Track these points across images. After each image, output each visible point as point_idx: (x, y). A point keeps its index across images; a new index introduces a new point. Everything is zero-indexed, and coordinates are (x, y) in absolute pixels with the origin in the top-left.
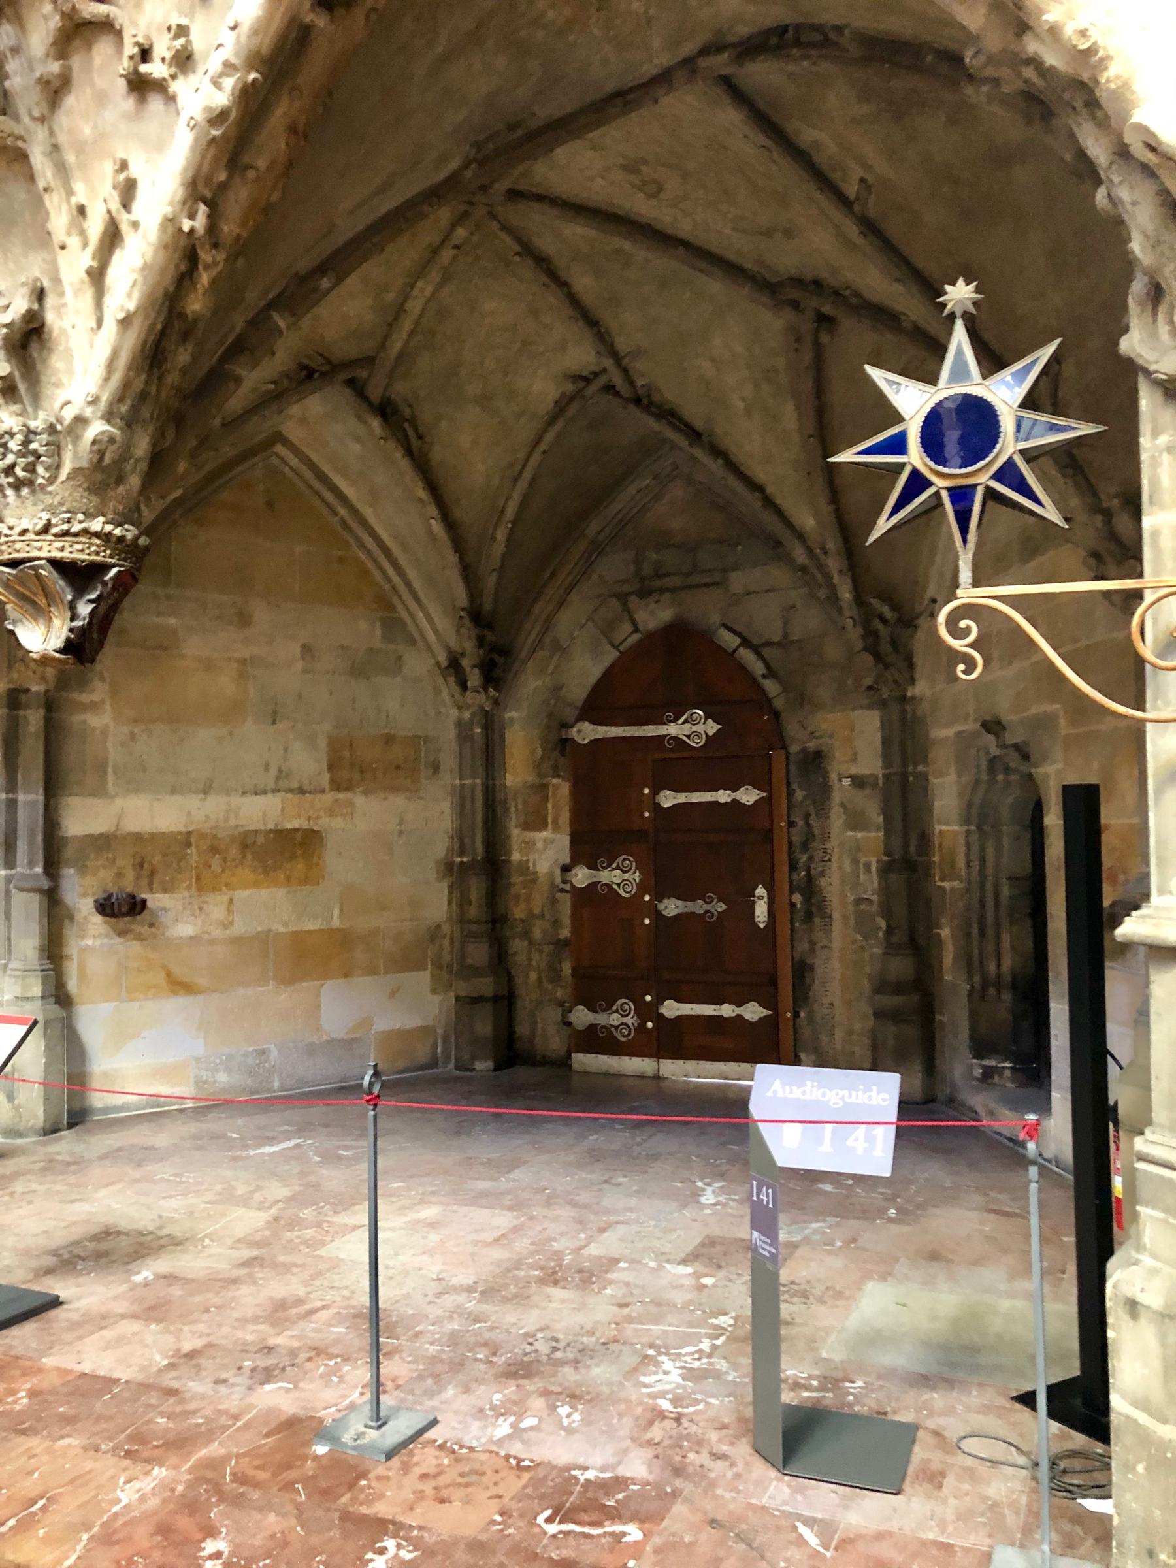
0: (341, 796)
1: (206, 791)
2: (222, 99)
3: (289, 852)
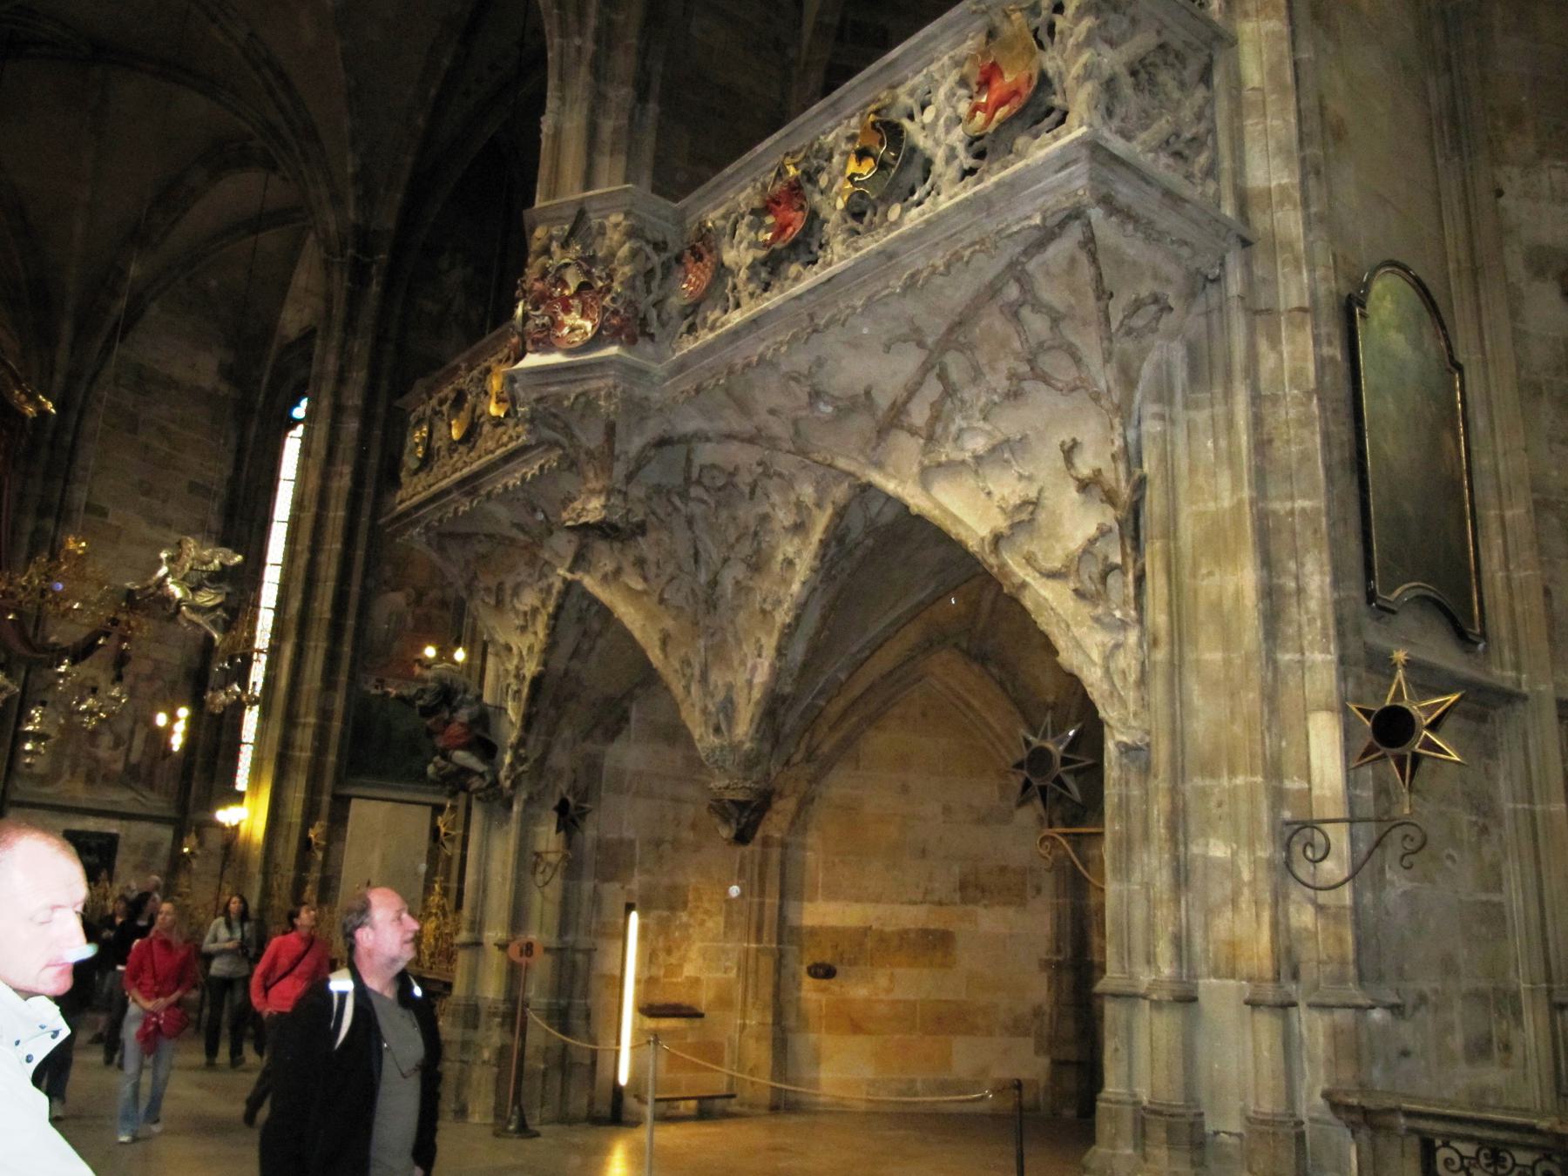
0: (970, 907)
1: (877, 900)
3: (933, 945)
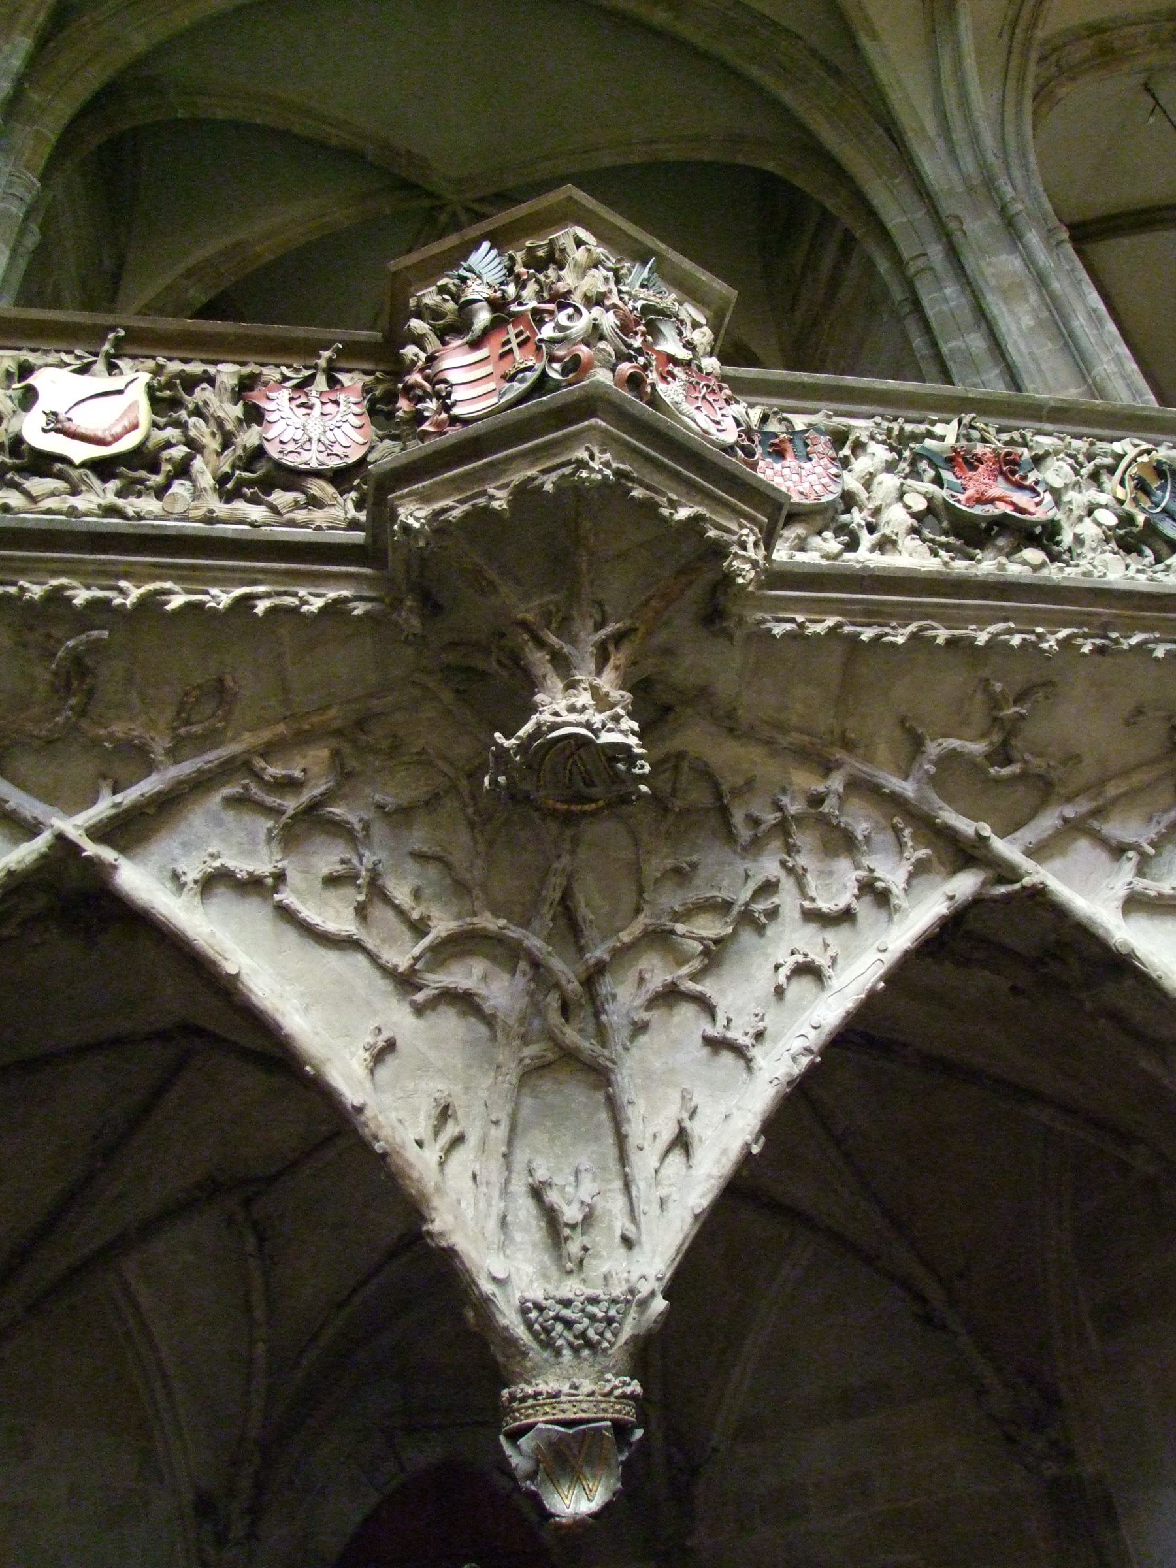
2: (796, 1071)
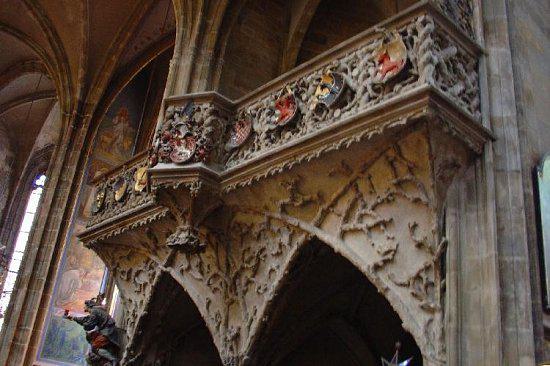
2: (271, 298)
